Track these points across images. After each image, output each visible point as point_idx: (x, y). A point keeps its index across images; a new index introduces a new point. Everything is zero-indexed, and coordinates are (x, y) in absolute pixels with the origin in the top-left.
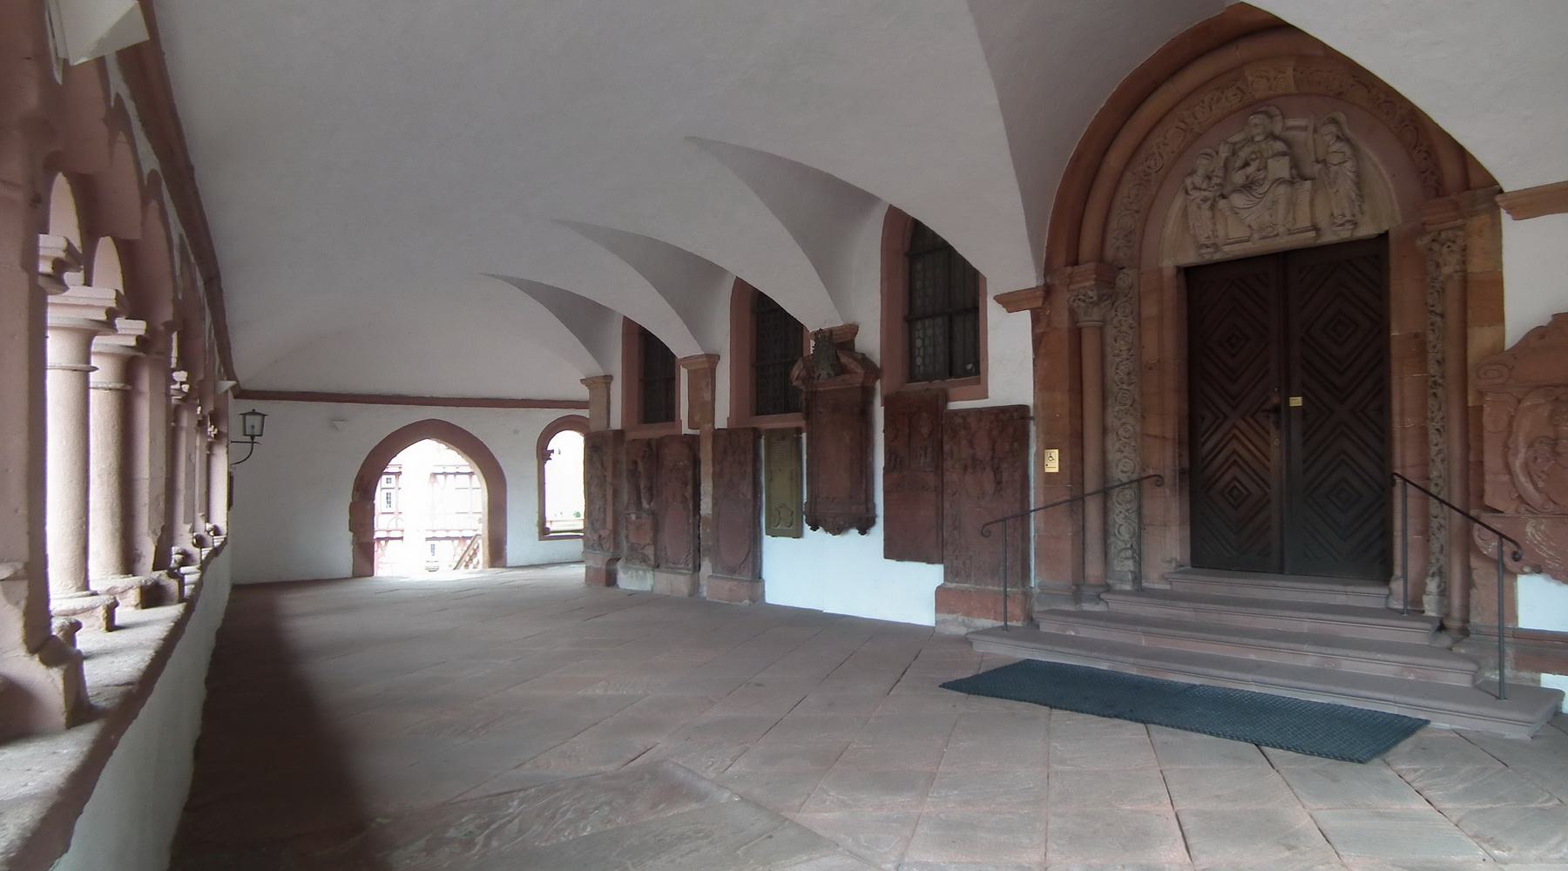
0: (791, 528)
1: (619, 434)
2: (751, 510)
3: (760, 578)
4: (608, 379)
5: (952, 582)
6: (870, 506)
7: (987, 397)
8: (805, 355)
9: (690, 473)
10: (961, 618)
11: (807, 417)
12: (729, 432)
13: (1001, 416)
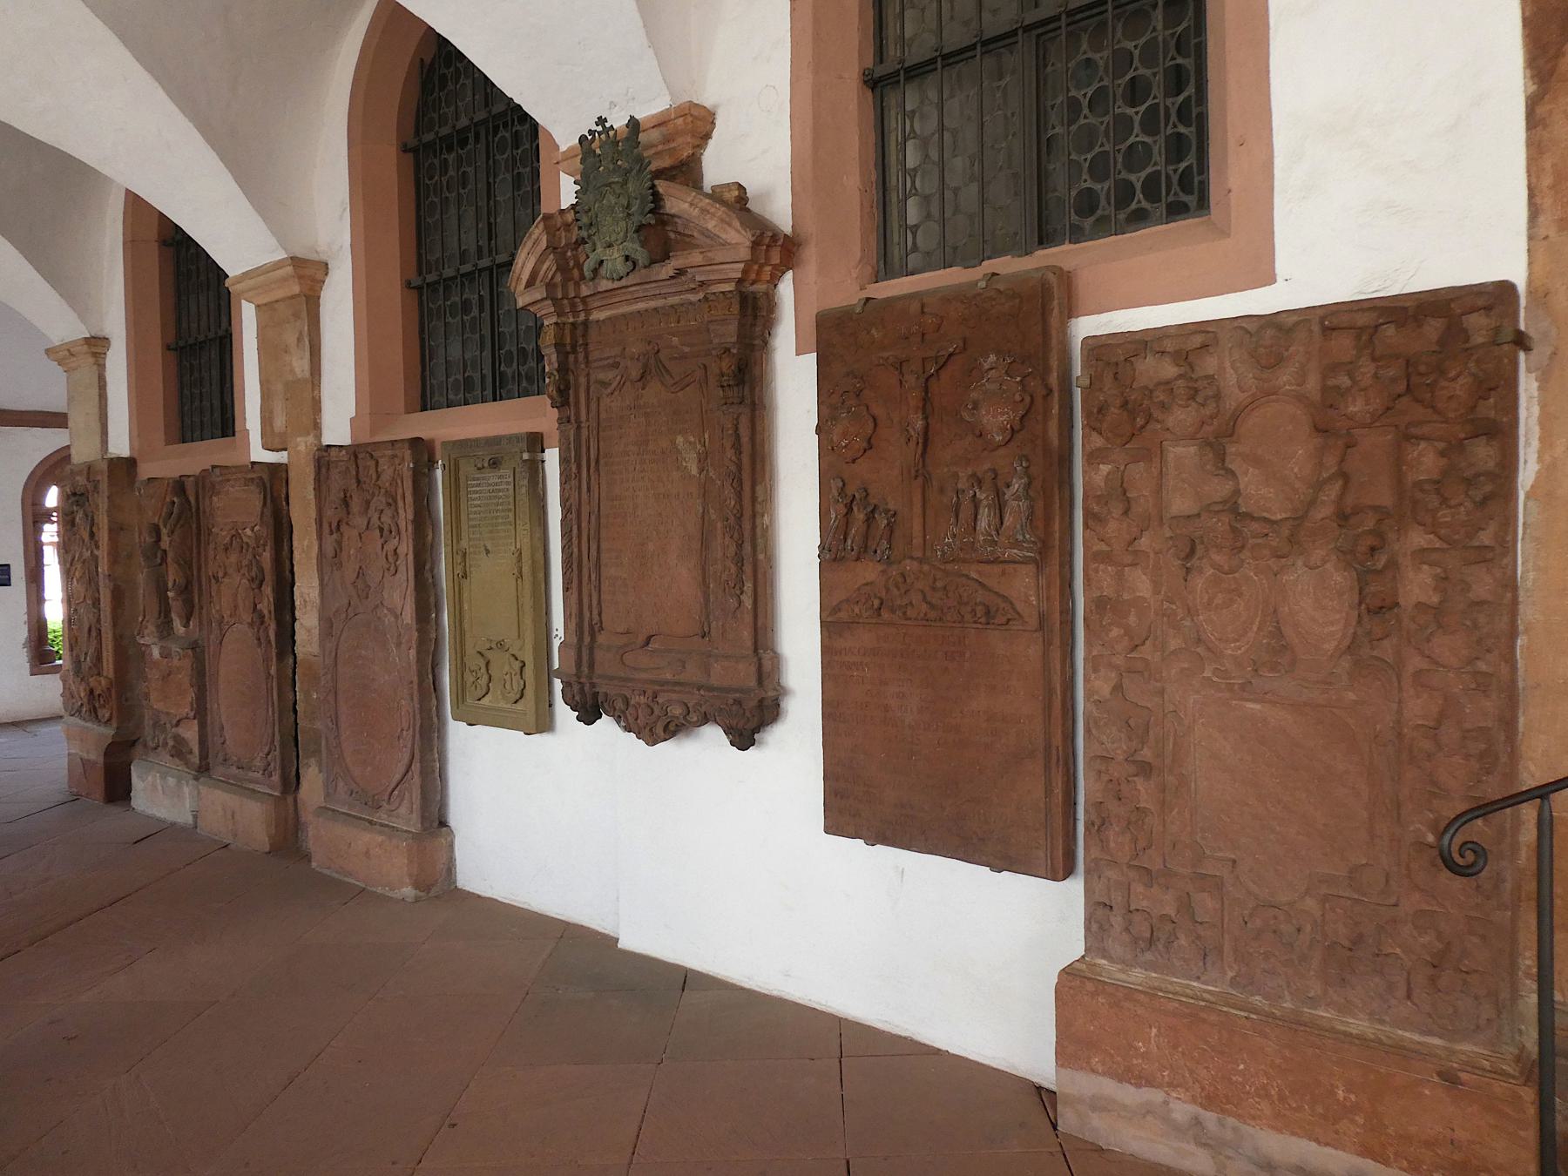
0: (519, 706)
1: (129, 464)
2: (413, 652)
4: (97, 345)
5: (1127, 964)
6: (767, 665)
7: (1270, 279)
8: (546, 207)
9: (267, 557)
10: (1182, 1110)
11: (563, 400)
12: (354, 452)
13: (1390, 330)
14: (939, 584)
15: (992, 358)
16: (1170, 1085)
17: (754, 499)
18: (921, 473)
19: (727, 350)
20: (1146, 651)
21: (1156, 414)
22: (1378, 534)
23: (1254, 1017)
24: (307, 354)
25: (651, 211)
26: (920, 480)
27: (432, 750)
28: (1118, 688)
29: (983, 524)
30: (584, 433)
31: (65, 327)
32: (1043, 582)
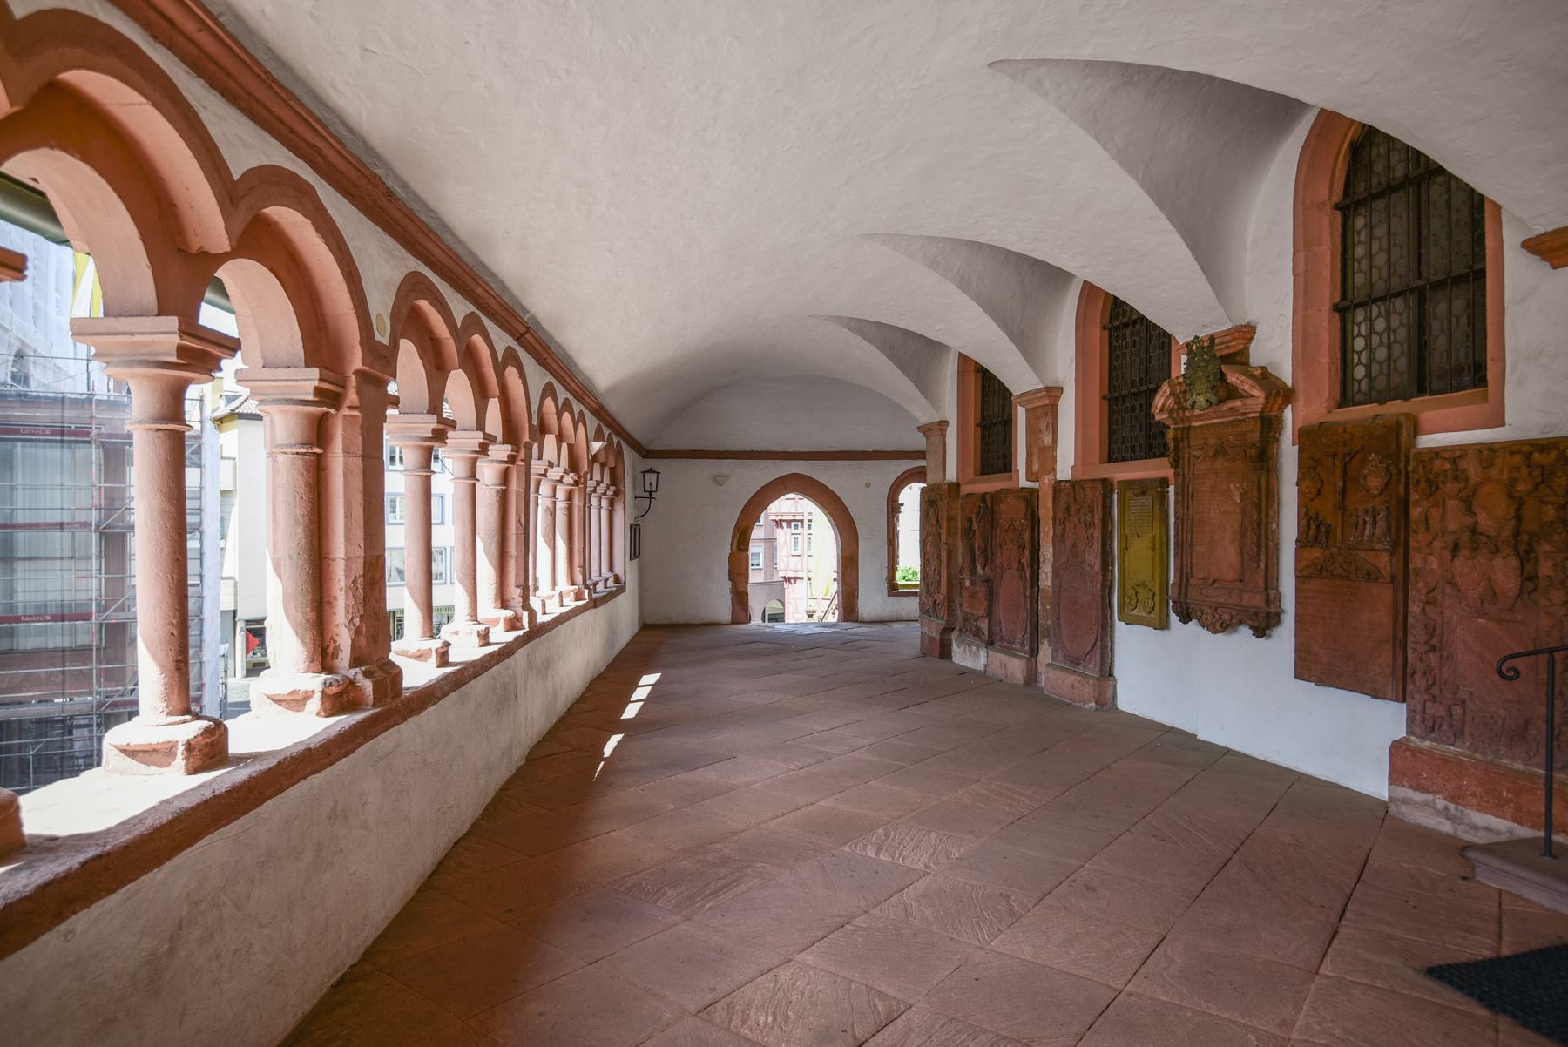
0: (1152, 615)
1: (957, 485)
2: (1099, 586)
3: (1111, 675)
4: (943, 424)
5: (1423, 738)
7: (1503, 424)
9: (1027, 535)
10: (1440, 803)
11: (1176, 464)
12: (1074, 484)
13: (1536, 455)
14: (1348, 560)
15: (1373, 455)
16: (1435, 792)
17: (1267, 515)
18: (1342, 507)
19: (1254, 445)
20: (1437, 594)
21: (1441, 486)
22: (1529, 544)
23: (1473, 761)
24: (1051, 434)
25: (1219, 379)
26: (1341, 511)
27: (1106, 635)
28: (1423, 610)
29: (1367, 532)
30: (1187, 480)
31: (925, 415)
32: (1394, 560)
